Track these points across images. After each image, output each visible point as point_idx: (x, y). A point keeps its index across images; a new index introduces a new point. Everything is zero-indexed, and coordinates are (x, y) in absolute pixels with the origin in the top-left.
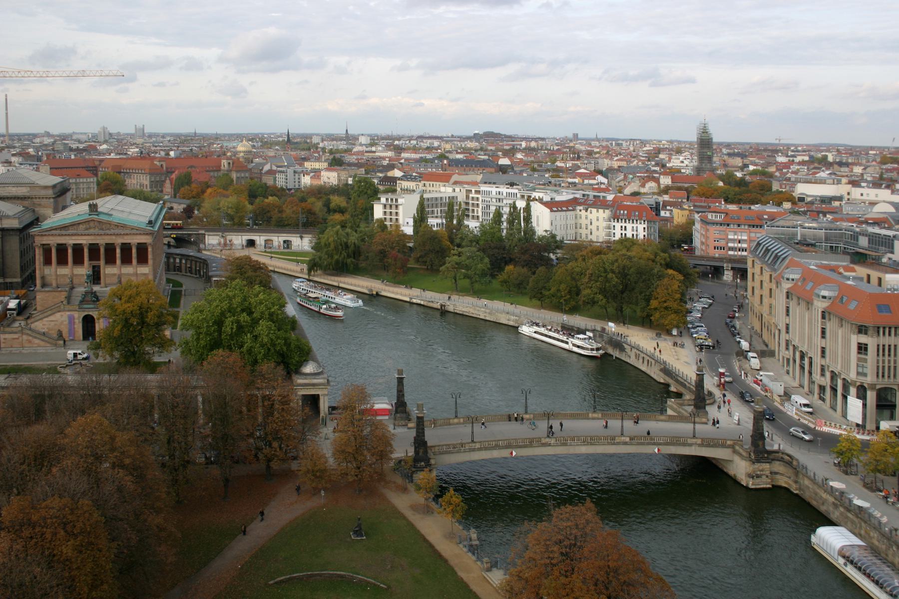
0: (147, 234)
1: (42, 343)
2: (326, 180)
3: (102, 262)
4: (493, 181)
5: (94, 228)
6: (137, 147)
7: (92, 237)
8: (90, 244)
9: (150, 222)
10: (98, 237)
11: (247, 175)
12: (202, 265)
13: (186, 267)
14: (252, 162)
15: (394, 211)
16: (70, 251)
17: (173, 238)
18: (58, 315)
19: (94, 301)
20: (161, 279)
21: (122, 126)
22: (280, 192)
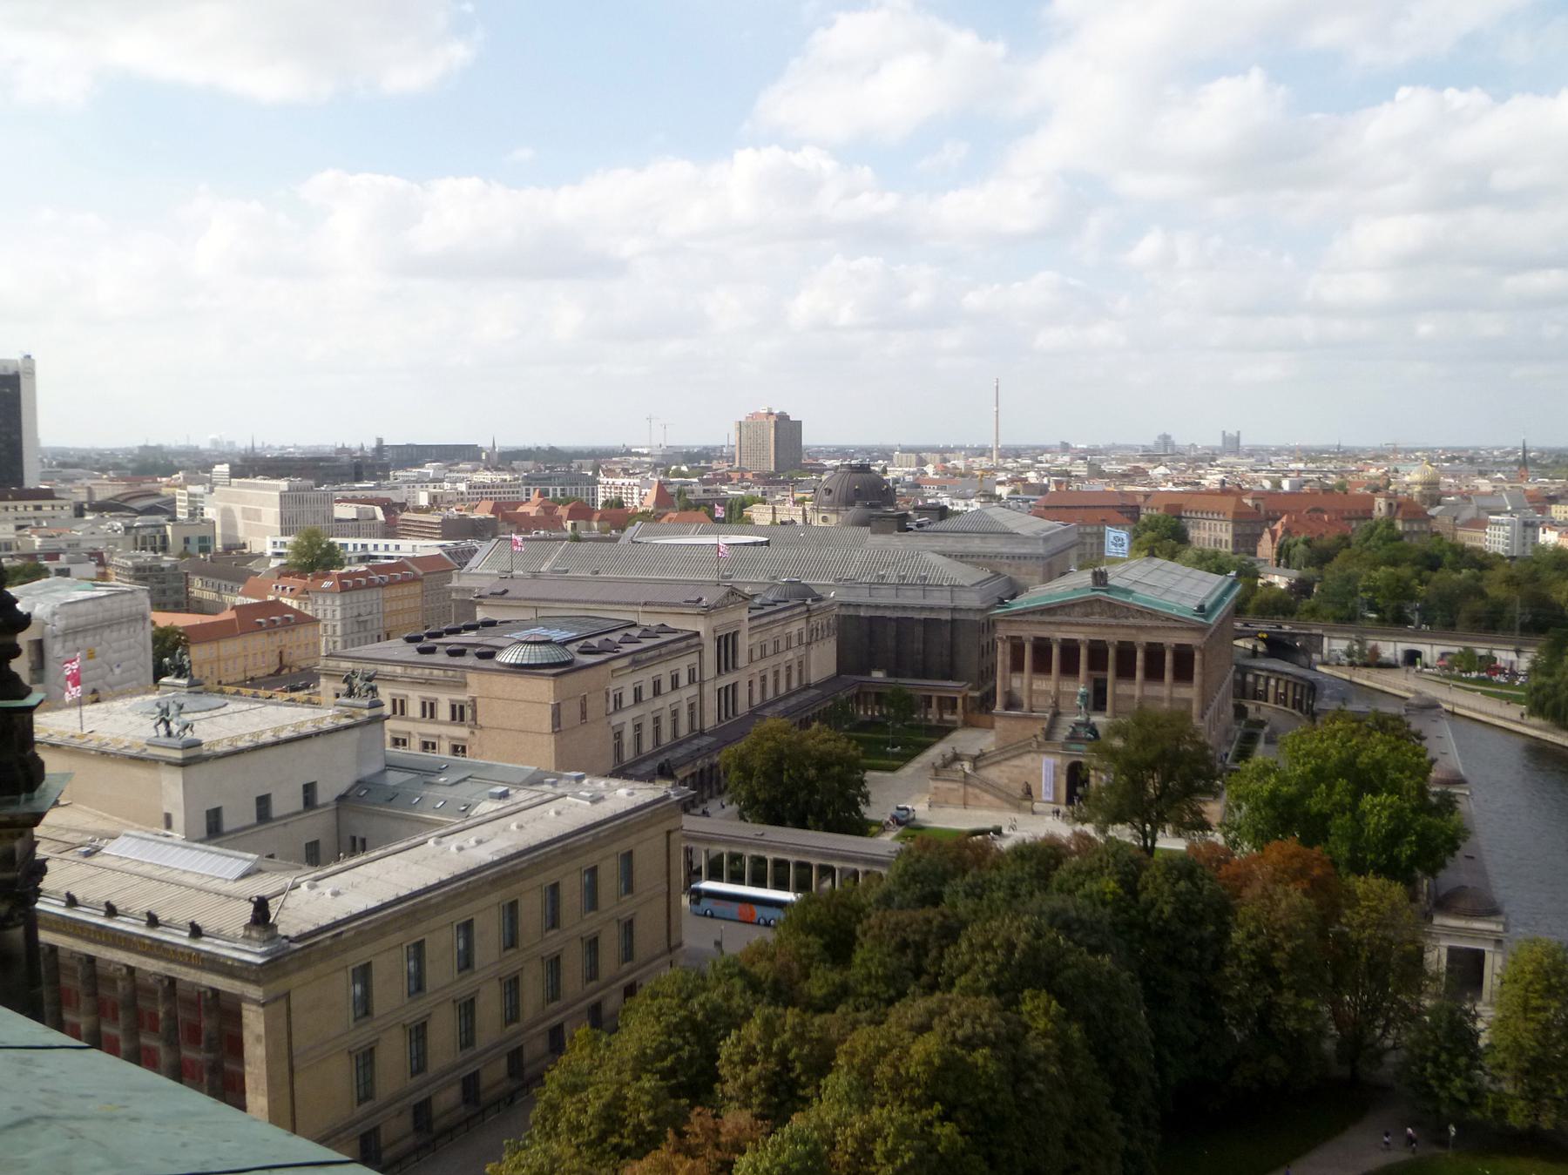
0: (1193, 629)
1: (997, 802)
3: (1110, 674)
5: (1101, 614)
6: (1221, 472)
7: (1096, 630)
8: (1092, 641)
9: (1201, 608)
10: (1105, 630)
11: (1424, 527)
12: (1305, 691)
14: (1439, 504)
16: (1056, 651)
17: (1262, 639)
18: (1027, 760)
19: (1090, 739)
20: (1219, 711)
21: (1198, 433)
22: (1481, 562)
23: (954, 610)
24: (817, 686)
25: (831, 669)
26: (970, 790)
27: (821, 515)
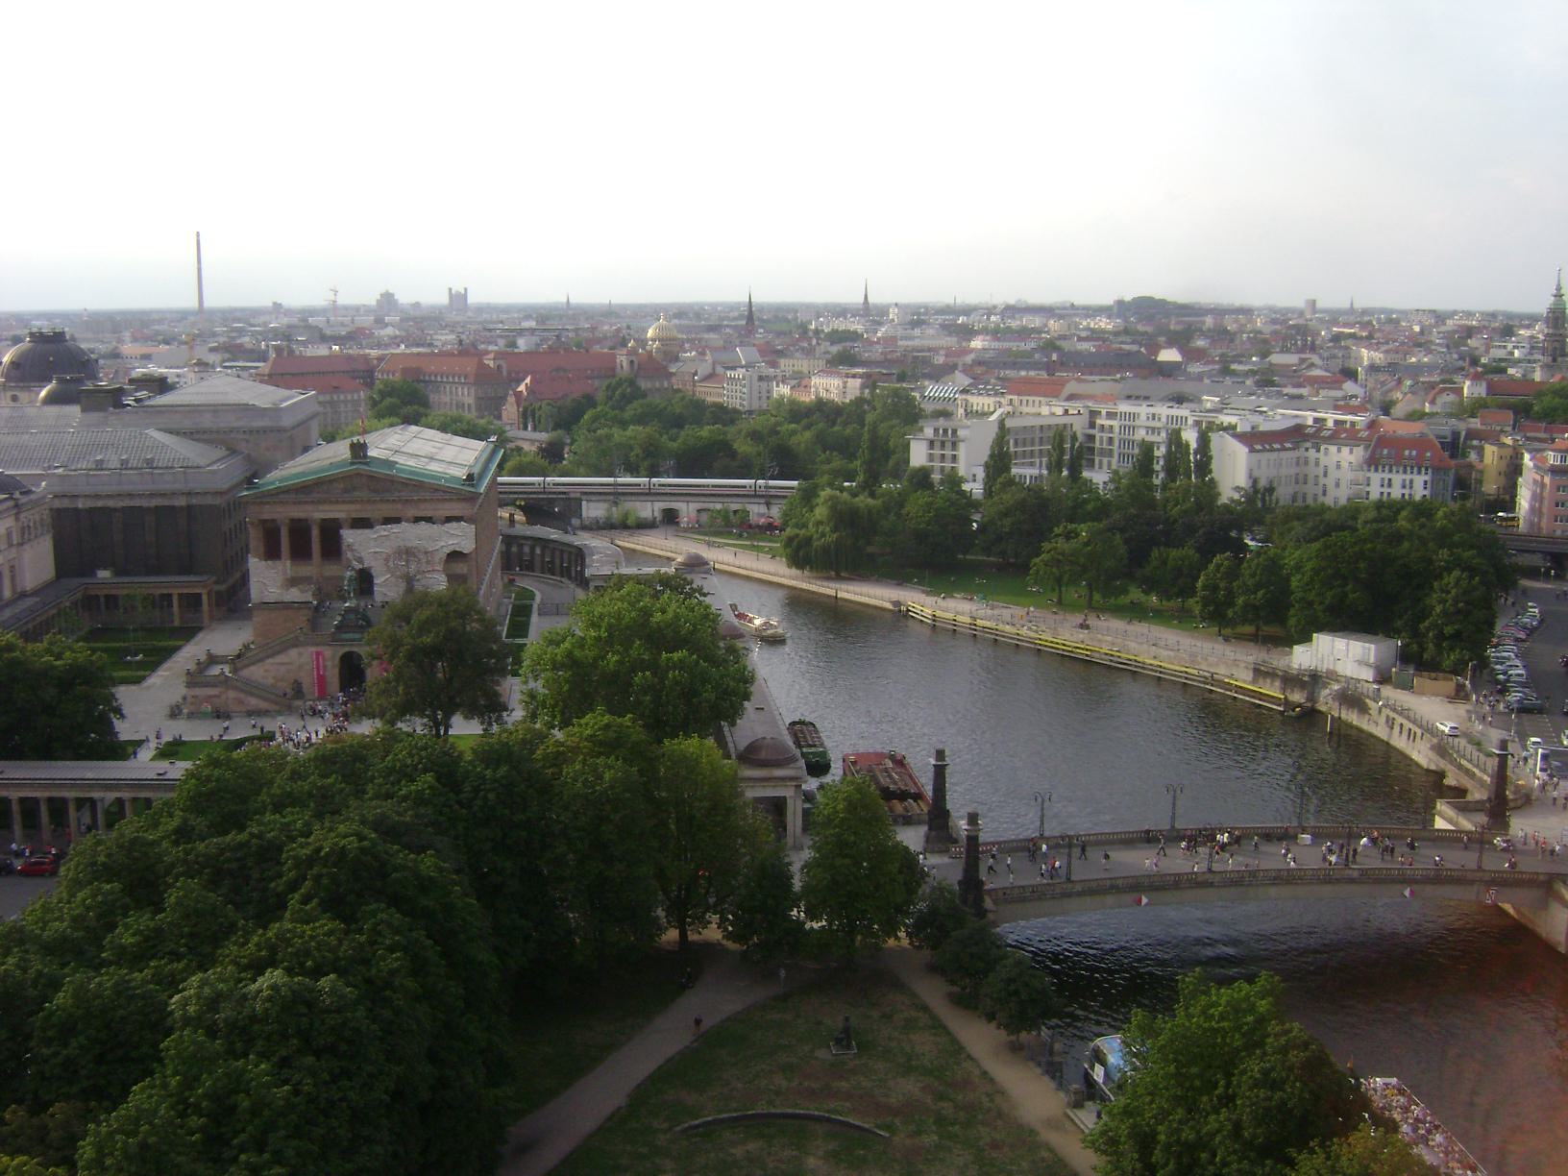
0: (464, 499)
2: (823, 394)
4: (1143, 393)
12: (573, 557)
13: (543, 561)
15: (948, 452)
19: (362, 627)
23: (189, 494)
24: (35, 593)
25: (48, 572)
26: (232, 694)
27: (9, 394)
